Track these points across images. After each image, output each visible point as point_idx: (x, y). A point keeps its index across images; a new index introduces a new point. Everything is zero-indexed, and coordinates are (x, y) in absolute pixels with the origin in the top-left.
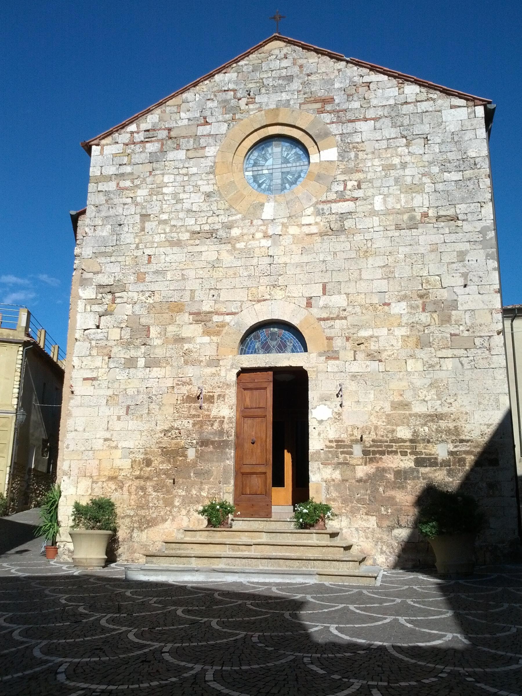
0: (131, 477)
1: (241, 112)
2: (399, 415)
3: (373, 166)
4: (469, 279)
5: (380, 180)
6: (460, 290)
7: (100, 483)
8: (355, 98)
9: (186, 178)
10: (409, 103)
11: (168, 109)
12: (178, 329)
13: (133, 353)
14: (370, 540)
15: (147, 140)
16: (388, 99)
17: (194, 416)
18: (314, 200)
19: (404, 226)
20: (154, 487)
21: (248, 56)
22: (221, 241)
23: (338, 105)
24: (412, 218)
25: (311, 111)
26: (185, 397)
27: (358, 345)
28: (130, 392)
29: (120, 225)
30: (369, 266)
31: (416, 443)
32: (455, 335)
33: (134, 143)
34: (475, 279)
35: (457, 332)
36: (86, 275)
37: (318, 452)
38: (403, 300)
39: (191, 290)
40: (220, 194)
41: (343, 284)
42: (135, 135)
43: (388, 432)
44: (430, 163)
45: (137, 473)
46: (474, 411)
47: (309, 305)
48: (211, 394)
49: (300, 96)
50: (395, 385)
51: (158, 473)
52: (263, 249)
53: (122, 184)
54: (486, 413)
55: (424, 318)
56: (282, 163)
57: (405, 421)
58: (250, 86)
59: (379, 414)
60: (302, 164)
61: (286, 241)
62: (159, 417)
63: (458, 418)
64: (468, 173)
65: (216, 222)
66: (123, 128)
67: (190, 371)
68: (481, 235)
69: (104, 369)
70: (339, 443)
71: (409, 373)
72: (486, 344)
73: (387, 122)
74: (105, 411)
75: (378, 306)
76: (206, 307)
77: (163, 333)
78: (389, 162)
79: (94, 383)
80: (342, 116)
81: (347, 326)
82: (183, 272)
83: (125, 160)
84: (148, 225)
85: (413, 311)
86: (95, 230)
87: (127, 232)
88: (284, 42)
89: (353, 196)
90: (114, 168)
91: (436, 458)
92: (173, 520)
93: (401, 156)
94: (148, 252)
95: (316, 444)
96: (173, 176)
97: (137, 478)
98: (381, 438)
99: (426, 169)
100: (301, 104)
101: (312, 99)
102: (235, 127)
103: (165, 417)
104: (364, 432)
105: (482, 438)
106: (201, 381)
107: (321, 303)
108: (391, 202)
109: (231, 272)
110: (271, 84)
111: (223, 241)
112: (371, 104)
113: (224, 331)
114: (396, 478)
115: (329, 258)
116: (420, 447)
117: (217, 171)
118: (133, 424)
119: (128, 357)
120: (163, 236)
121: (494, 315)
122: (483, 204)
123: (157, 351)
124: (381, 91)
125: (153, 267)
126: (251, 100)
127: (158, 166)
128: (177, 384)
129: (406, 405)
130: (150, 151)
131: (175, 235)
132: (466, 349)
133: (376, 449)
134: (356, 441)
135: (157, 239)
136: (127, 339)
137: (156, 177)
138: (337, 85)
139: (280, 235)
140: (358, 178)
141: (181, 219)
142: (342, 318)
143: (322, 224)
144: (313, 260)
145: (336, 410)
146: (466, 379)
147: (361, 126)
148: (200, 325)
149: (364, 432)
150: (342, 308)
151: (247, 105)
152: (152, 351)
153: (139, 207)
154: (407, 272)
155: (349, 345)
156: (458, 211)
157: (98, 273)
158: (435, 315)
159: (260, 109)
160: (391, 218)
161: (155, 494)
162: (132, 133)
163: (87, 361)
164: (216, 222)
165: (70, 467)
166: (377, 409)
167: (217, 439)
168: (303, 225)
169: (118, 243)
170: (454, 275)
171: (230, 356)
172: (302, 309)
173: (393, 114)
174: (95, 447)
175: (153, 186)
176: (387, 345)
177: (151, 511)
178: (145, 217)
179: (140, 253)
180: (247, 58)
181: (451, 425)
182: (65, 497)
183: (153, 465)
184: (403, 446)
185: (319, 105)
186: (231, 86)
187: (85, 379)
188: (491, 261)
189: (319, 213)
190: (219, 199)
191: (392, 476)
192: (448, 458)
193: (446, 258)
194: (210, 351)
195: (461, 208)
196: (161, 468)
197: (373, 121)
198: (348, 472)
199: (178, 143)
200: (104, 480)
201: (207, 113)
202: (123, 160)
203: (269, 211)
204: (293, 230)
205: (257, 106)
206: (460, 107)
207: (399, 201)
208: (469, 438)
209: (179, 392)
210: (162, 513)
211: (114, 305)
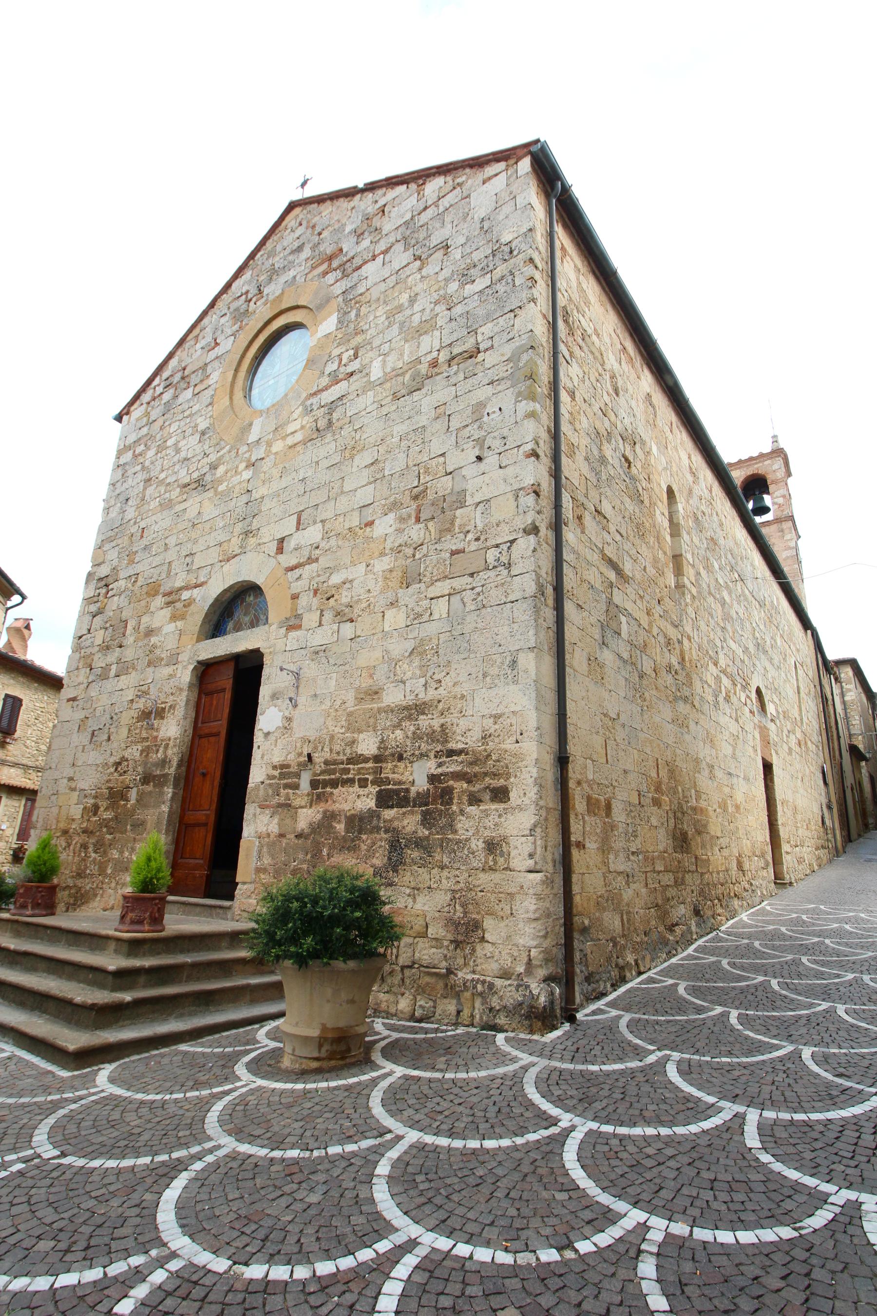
4: (486, 446)
18: (304, 395)
19: (403, 392)
34: (497, 444)
35: (460, 546)
37: (257, 788)
38: (391, 510)
45: (85, 825)
54: (493, 692)
55: (416, 532)
61: (266, 465)
71: (385, 635)
84: (150, 491)
85: (403, 526)
91: (407, 790)
94: (143, 524)
95: (258, 774)
98: (335, 756)
99: (442, 292)
108: (392, 361)
114: (347, 831)
129: (376, 693)
132: (472, 575)
133: (327, 777)
145: (287, 714)
147: (369, 269)
149: (316, 748)
155: (315, 602)
158: (430, 524)
161: (93, 855)
166: (338, 703)
170: (465, 446)
181: (436, 724)
185: (325, 266)
198: (288, 821)
208: (464, 746)
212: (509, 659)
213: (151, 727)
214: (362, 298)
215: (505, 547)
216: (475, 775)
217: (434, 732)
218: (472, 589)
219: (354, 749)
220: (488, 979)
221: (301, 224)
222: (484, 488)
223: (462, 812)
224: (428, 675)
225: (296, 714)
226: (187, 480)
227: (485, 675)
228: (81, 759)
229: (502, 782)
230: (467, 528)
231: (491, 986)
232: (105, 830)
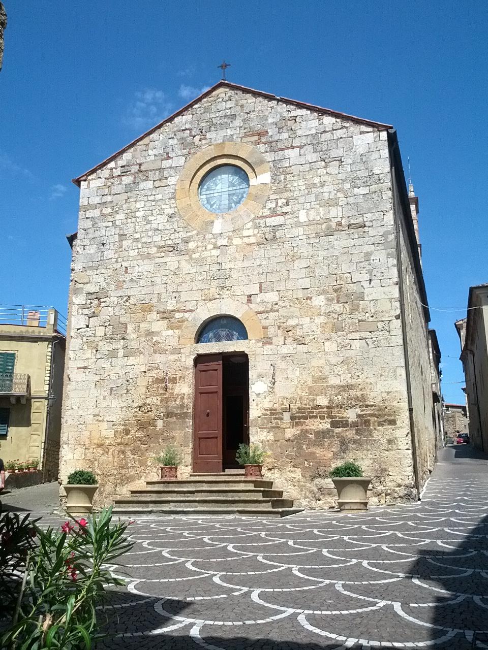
0: (114, 444)
1: (196, 147)
3: (298, 185)
4: (373, 275)
5: (304, 197)
7: (91, 450)
8: (285, 130)
9: (153, 204)
10: (328, 132)
11: (139, 148)
12: (149, 325)
13: (115, 346)
14: (296, 487)
15: (123, 174)
18: (253, 216)
19: (322, 234)
23: (271, 137)
25: (250, 143)
26: (154, 379)
27: (287, 332)
29: (103, 244)
30: (296, 268)
31: (331, 409)
32: (363, 321)
34: (378, 274)
35: (364, 318)
36: (78, 286)
37: (256, 419)
38: (321, 294)
39: (158, 294)
40: (180, 214)
41: (275, 283)
42: (114, 170)
45: (119, 440)
46: (376, 381)
47: (249, 301)
48: (174, 376)
50: (315, 362)
51: (135, 440)
53: (104, 212)
54: (386, 383)
55: (338, 307)
56: (229, 187)
57: (323, 391)
58: (203, 125)
60: (244, 187)
61: (231, 250)
63: (364, 388)
64: (374, 187)
65: (177, 237)
66: (104, 166)
67: (158, 358)
68: (383, 238)
69: (92, 360)
70: (272, 411)
71: (326, 353)
73: (310, 148)
74: (94, 392)
75: (302, 300)
76: (170, 307)
77: (137, 329)
78: (312, 182)
79: (85, 370)
80: (273, 146)
82: (153, 279)
83: (106, 191)
85: (329, 303)
86: (84, 249)
87: (109, 249)
89: (283, 211)
90: (99, 198)
91: (347, 421)
94: (125, 264)
95: (254, 412)
99: (340, 186)
101: (251, 133)
102: (191, 160)
103: (139, 395)
104: (291, 402)
105: (383, 403)
107: (259, 299)
108: (312, 214)
109: (189, 277)
110: (218, 123)
112: (297, 134)
114: (316, 437)
115: (264, 263)
116: (335, 412)
117: (177, 197)
118: (115, 402)
120: (136, 251)
121: (393, 303)
122: (385, 213)
123: (132, 343)
124: (305, 123)
125: (130, 276)
126: (203, 137)
128: (149, 370)
131: (146, 250)
132: (370, 332)
133: (301, 415)
134: (285, 410)
135: (132, 253)
138: (270, 120)
139: (226, 246)
141: (150, 237)
143: (259, 235)
148: (166, 321)
150: (274, 303)
151: (200, 141)
155: (280, 332)
157: (87, 283)
158: (346, 305)
159: (210, 144)
160: (312, 227)
161: (133, 456)
162: (111, 169)
164: (177, 238)
165: (68, 438)
167: (179, 412)
168: (244, 237)
169: (102, 258)
170: (361, 272)
173: (315, 142)
177: (130, 470)
178: (122, 236)
181: (359, 394)
183: (131, 434)
185: (256, 138)
186: (187, 126)
187: (78, 368)
189: (257, 226)
190: (178, 219)
191: (313, 436)
192: (356, 420)
193: (355, 259)
194: (173, 342)
195: (368, 216)
196: (137, 436)
197: (298, 149)
199: (147, 175)
200: (94, 447)
201: (169, 150)
202: (105, 192)
203: (217, 228)
204: (237, 241)
205: (209, 141)
206: (368, 132)
207: (319, 213)
208: (373, 403)
209: (150, 375)
211: (100, 308)
214: (288, 170)
215: (387, 322)
216: (380, 415)
218: (372, 338)
220: (392, 488)
223: (375, 429)
228: (104, 404)
229: (393, 418)
230: (366, 311)
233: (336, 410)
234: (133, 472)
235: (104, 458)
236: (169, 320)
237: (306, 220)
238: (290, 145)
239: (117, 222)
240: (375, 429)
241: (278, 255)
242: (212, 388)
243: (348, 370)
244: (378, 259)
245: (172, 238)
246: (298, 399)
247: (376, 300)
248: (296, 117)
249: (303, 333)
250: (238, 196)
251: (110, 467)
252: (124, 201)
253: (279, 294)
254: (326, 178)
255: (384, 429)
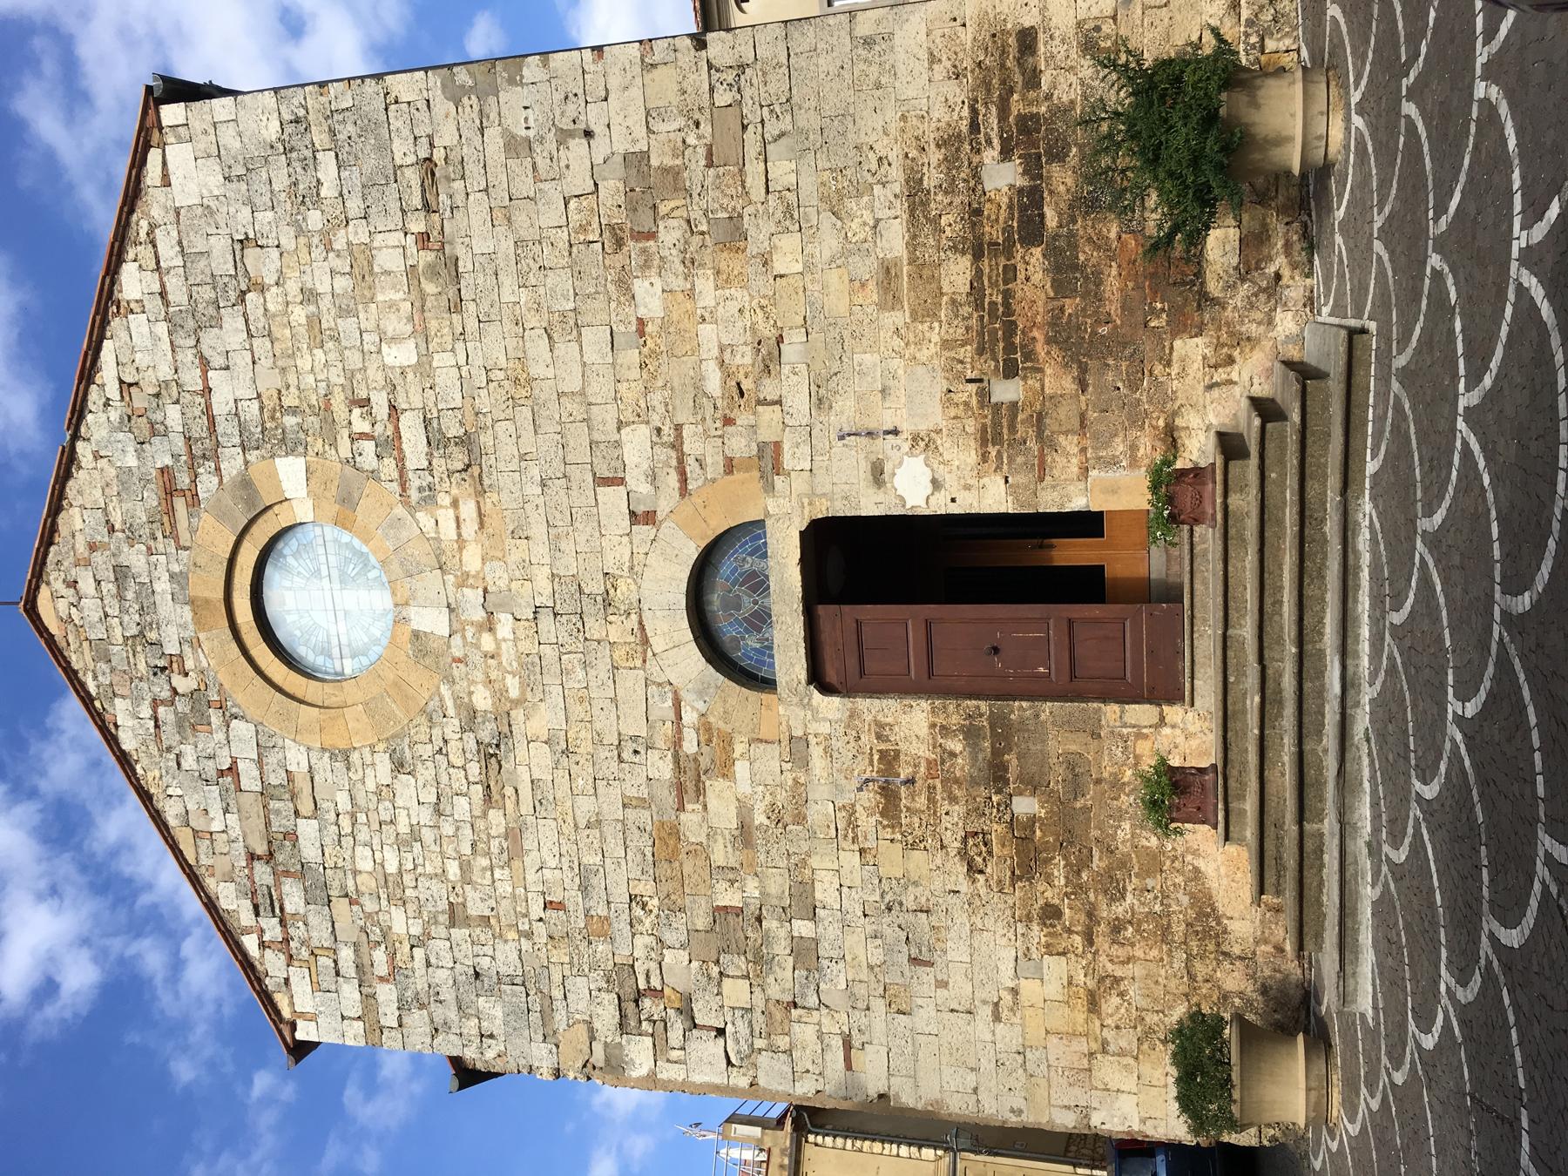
0: (1090, 956)
2: (912, 288)
3: (315, 370)
4: (572, 126)
5: (347, 352)
6: (601, 147)
8: (158, 417)
9: (362, 818)
10: (163, 285)
11: (204, 861)
12: (719, 838)
13: (781, 948)
14: (1236, 353)
15: (277, 911)
16: (156, 339)
17: (931, 800)
18: (400, 510)
19: (452, 292)
20: (1113, 899)
21: (75, 672)
22: (503, 737)
24: (433, 272)
27: (742, 394)
28: (876, 956)
29: (477, 975)
31: (981, 245)
32: (709, 155)
33: (287, 940)
34: (571, 109)
35: (702, 151)
36: (599, 1057)
39: (624, 806)
40: (394, 736)
41: (597, 436)
43: (957, 316)
44: (300, 232)
45: (1078, 940)
47: (649, 518)
48: (876, 757)
49: (161, 548)
50: (837, 299)
52: (521, 634)
53: (382, 969)
54: (901, 70)
55: (670, 234)
58: (142, 666)
59: (912, 339)
61: (498, 577)
62: (937, 885)
63: (917, 138)
64: (319, 137)
65: (460, 745)
66: (252, 967)
67: (820, 811)
69: (824, 1020)
70: (987, 438)
71: (809, 267)
72: (730, 76)
73: (209, 338)
74: (925, 1017)
75: (645, 350)
76: (662, 768)
78: (302, 330)
79: (856, 1043)
81: (696, 424)
82: (582, 823)
83: (325, 961)
84: (476, 908)
85: (656, 263)
86: (491, 1036)
88: (38, 588)
91: (1021, 191)
92: (1196, 853)
93: (287, 304)
94: (536, 910)
96: (359, 849)
97: (1089, 939)
99: (315, 240)
100: (179, 547)
101: (166, 519)
102: (238, 702)
103: (936, 874)
106: (844, 782)
107: (644, 488)
108: (395, 324)
109: (578, 710)
111: (506, 729)
113: (721, 725)
115: (535, 472)
116: (993, 232)
117: (343, 745)
118: (956, 951)
119: (791, 959)
120: (498, 873)
121: (657, 58)
122: (390, 99)
123: (773, 889)
125: (573, 898)
126: (175, 666)
127: (336, 884)
130: (302, 903)
131: (495, 844)
132: (744, 127)
133: (1001, 345)
134: (984, 395)
135: (505, 888)
136: (748, 962)
137: (362, 888)
138: (131, 461)
139: (485, 591)
140: (343, 407)
141: (458, 829)
142: (679, 436)
143: (455, 491)
144: (541, 510)
145: (906, 447)
146: (816, 122)
148: (708, 783)
151: (186, 675)
152: (775, 902)
153: (434, 931)
154: (560, 281)
155: (743, 418)
156: (411, 159)
158: (663, 209)
159: (195, 644)
160: (433, 325)
161: (1129, 897)
162: (262, 945)
163: (804, 1060)
164: (462, 747)
165: (1067, 1108)
166: (897, 343)
168: (459, 535)
169: (518, 980)
170: (562, 164)
171: (781, 710)
172: (660, 535)
173: (191, 324)
174: (1016, 1044)
175: (384, 896)
176: (739, 324)
177: (1175, 908)
178: (455, 915)
179: (540, 928)
180: (80, 675)
181: (935, 156)
182: (1143, 1121)
183: (1056, 901)
184: (990, 278)
185: (180, 504)
186: (146, 711)
188: (525, 72)
189: (429, 495)
190: (407, 740)
193: (525, 186)
194: (771, 760)
195: (403, 150)
196: (1063, 882)
197: (210, 374)
199: (281, 837)
200: (1098, 1023)
201: (210, 768)
204: (472, 559)
205: (187, 649)
206: (164, 163)
207: (392, 306)
210: (1179, 880)
211: (667, 991)
212: (860, 51)
213: (910, 781)
214: (269, 404)
216: (1003, 82)
217: (946, 159)
219: (962, 298)
221: (73, 584)
222: (629, 122)
223: (1049, 97)
224: (871, 180)
225: (906, 427)
226: (478, 790)
227: (878, 86)
228: (960, 989)
229: (1012, 41)
230: (680, 144)
231: (1250, 23)
232: (1084, 875)
233: (987, 229)
234: (1180, 896)
235: (1133, 992)
236: (706, 772)
237: (411, 344)
238: (199, 399)
239: (413, 931)
240: (1049, 97)
241: (512, 429)
242: (914, 635)
243: (859, 195)
244: (524, 113)
245: (459, 762)
246: (952, 354)
247: (648, 114)
248: (121, 382)
249: (745, 344)
250: (347, 561)
251: (1163, 972)
252: (355, 908)
253: (628, 424)
254: (292, 287)
255: (1047, 65)
